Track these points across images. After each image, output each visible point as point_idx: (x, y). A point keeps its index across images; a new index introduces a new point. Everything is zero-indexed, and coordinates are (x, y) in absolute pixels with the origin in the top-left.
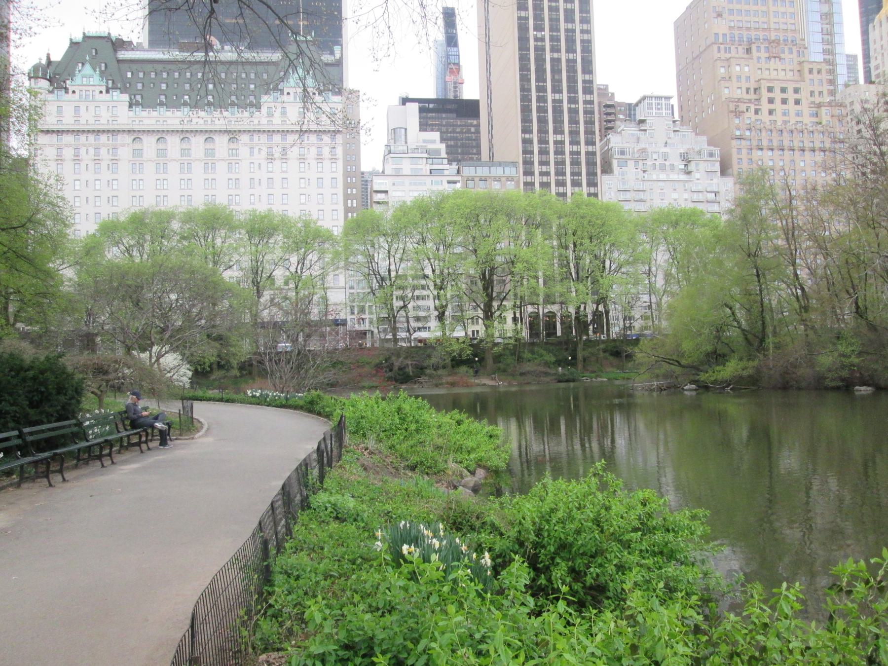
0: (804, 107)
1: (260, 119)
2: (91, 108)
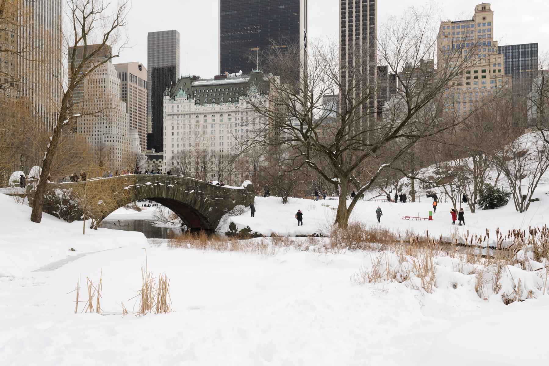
0: (488, 79)
2: (183, 106)
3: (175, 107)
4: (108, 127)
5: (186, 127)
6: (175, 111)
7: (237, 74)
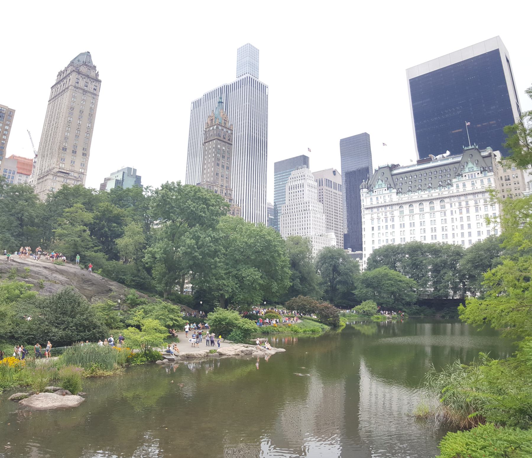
1: (453, 190)
2: (382, 197)
3: (374, 199)
4: (306, 228)
5: (389, 219)
6: (375, 203)
7: (445, 155)
